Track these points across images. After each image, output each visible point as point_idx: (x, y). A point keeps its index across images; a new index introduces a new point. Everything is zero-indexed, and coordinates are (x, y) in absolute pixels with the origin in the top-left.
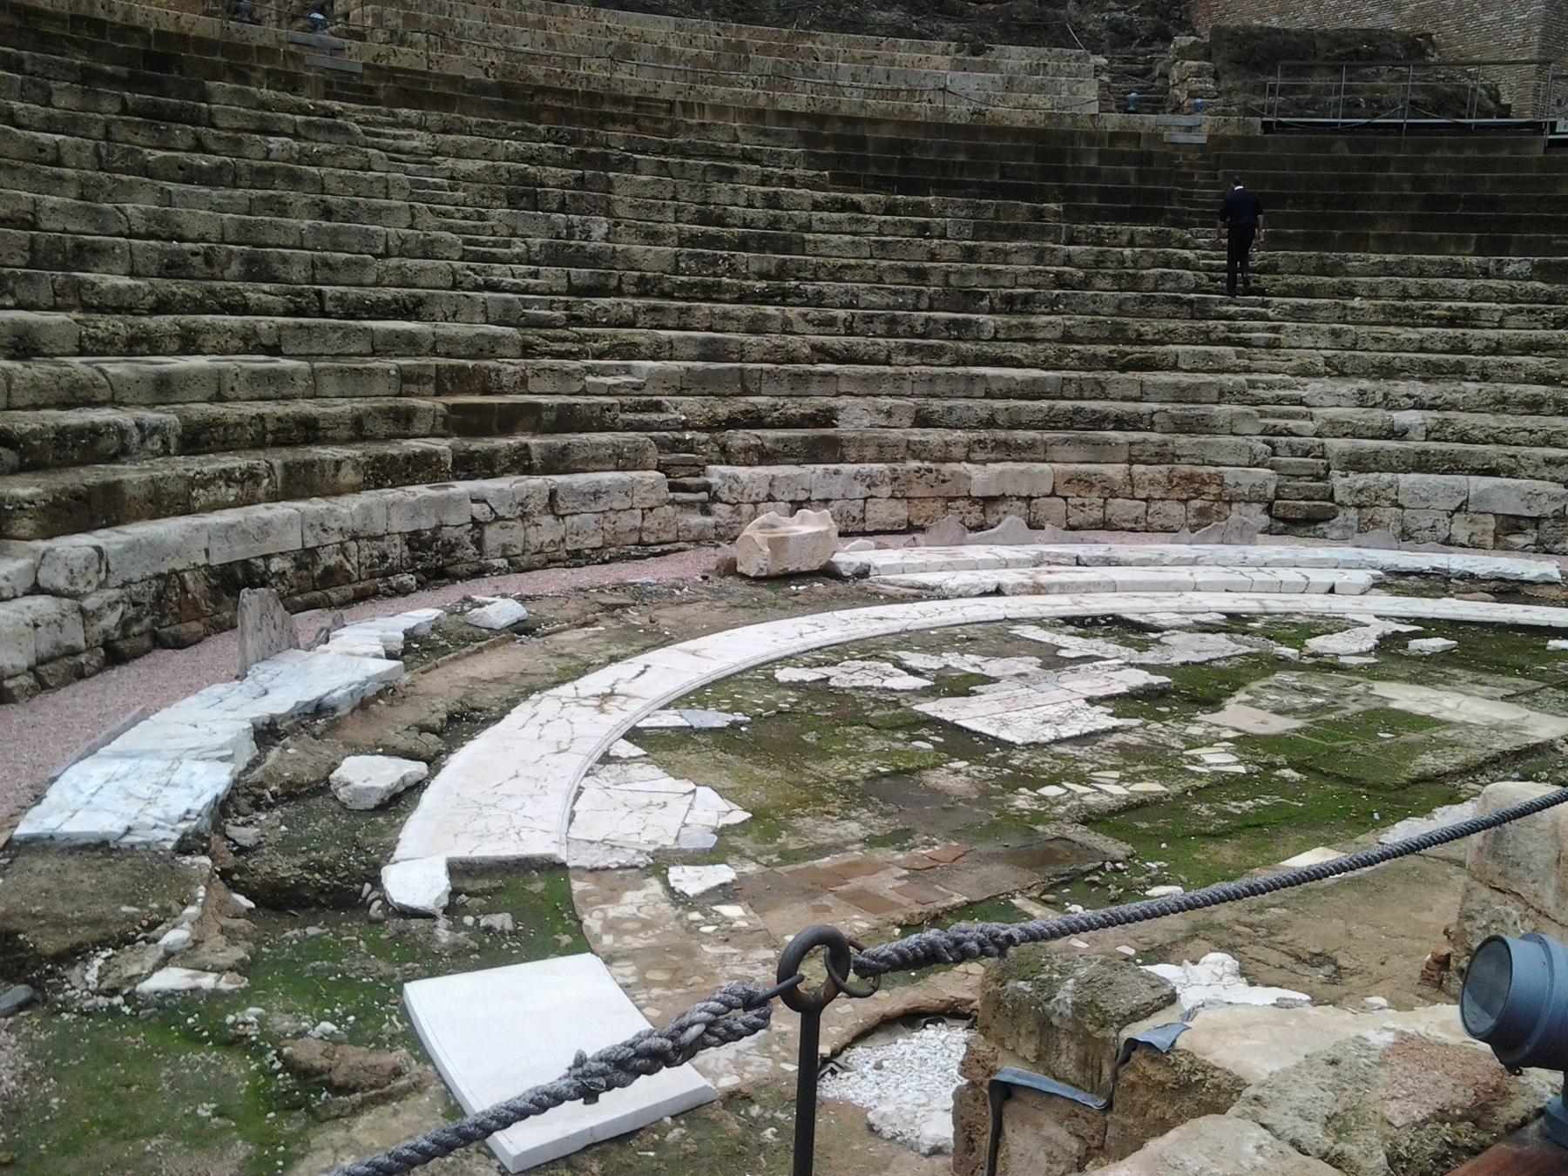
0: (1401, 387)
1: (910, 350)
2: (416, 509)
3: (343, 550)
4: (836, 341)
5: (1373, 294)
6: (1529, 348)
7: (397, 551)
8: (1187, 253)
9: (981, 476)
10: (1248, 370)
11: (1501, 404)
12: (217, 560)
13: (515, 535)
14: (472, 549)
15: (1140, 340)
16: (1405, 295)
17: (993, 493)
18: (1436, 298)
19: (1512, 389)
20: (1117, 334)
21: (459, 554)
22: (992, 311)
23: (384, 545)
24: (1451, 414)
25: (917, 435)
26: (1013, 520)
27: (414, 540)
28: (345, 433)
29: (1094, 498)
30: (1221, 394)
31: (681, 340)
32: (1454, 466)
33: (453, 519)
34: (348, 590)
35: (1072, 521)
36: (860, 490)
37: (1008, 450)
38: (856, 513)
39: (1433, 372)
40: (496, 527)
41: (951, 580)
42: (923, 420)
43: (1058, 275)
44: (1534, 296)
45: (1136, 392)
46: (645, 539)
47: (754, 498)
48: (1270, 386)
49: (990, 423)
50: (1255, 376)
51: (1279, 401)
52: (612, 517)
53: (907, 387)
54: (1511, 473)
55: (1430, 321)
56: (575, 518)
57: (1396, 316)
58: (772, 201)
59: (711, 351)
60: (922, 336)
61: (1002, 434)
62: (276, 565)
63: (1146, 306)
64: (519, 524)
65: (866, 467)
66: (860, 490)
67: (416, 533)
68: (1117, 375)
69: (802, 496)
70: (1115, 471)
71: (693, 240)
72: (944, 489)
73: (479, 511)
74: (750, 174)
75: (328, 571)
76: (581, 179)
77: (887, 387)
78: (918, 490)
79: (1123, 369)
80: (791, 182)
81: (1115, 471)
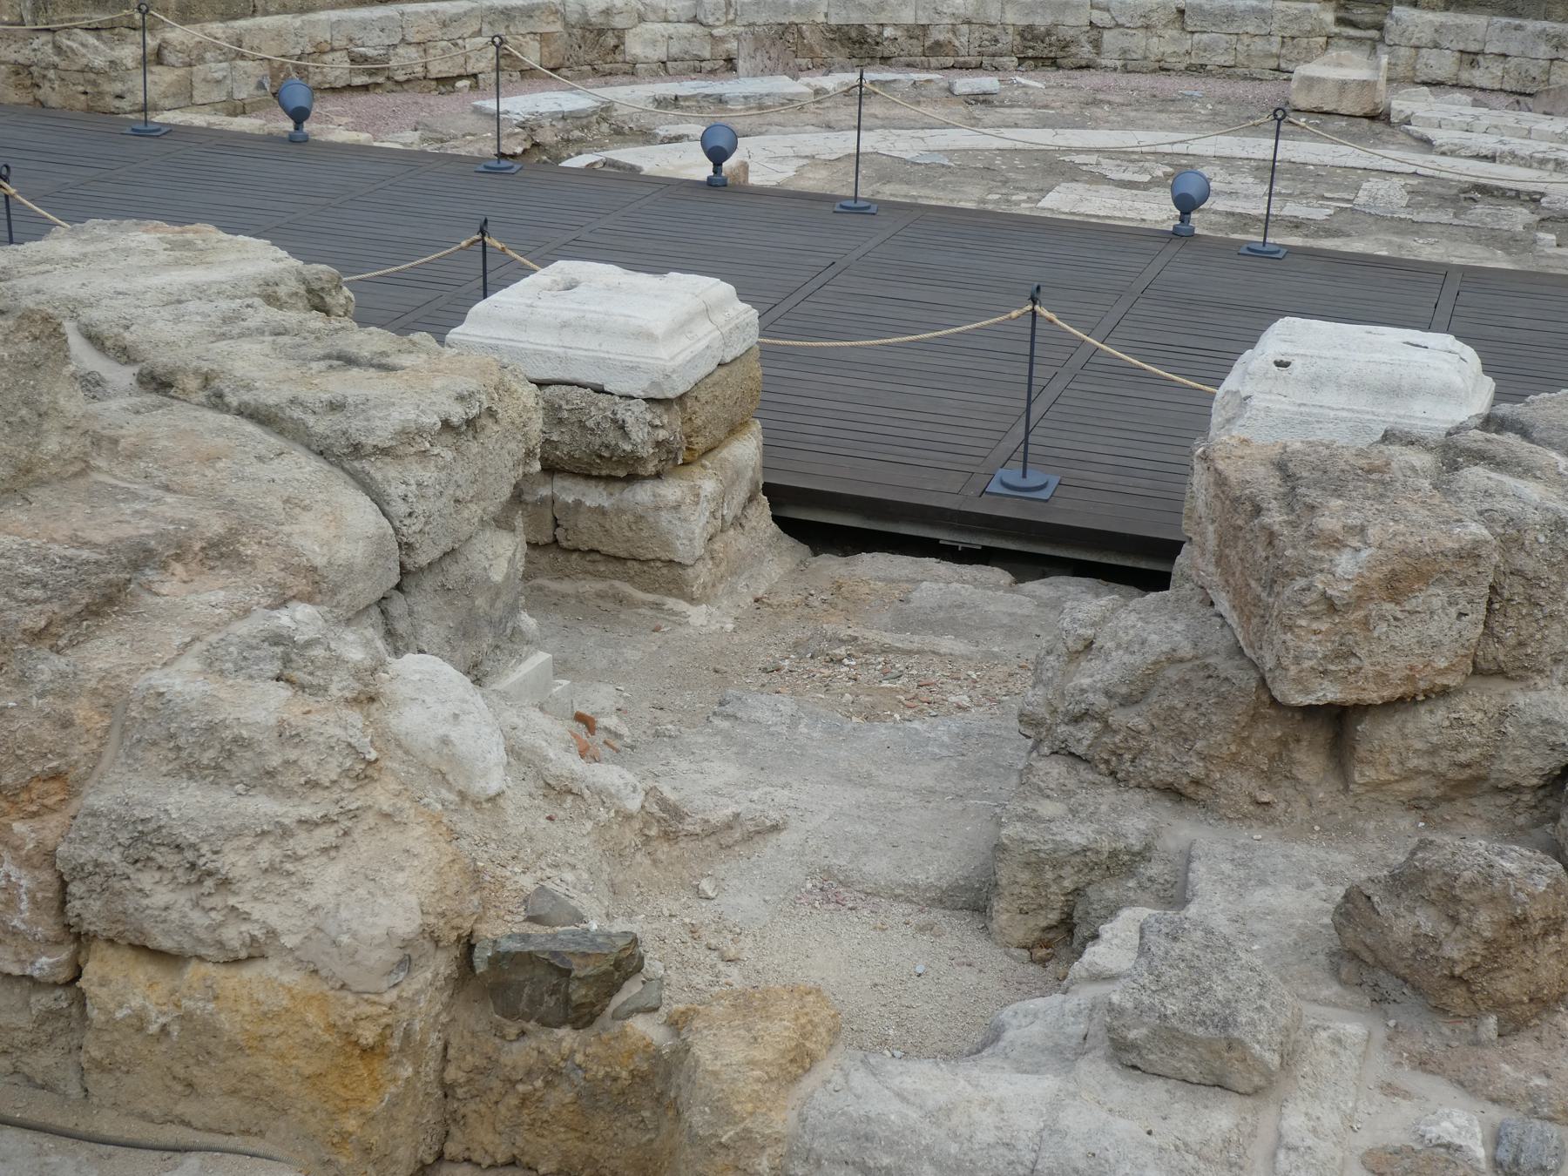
3: (954, 30)
7: (1009, 40)
12: (833, 21)
13: (1137, 41)
14: (1088, 47)
21: (1073, 50)
23: (995, 32)
27: (1028, 34)
33: (1070, 21)
34: (950, 61)
36: (1544, 50)
38: (1534, 72)
40: (1116, 32)
41: (1440, 137)
46: (1283, 66)
47: (1414, 42)
52: (1246, 39)
56: (1205, 36)
62: (888, 32)
64: (1140, 33)
66: (1544, 50)
67: (1030, 27)
69: (1473, 47)
73: (1097, 16)
75: (938, 44)
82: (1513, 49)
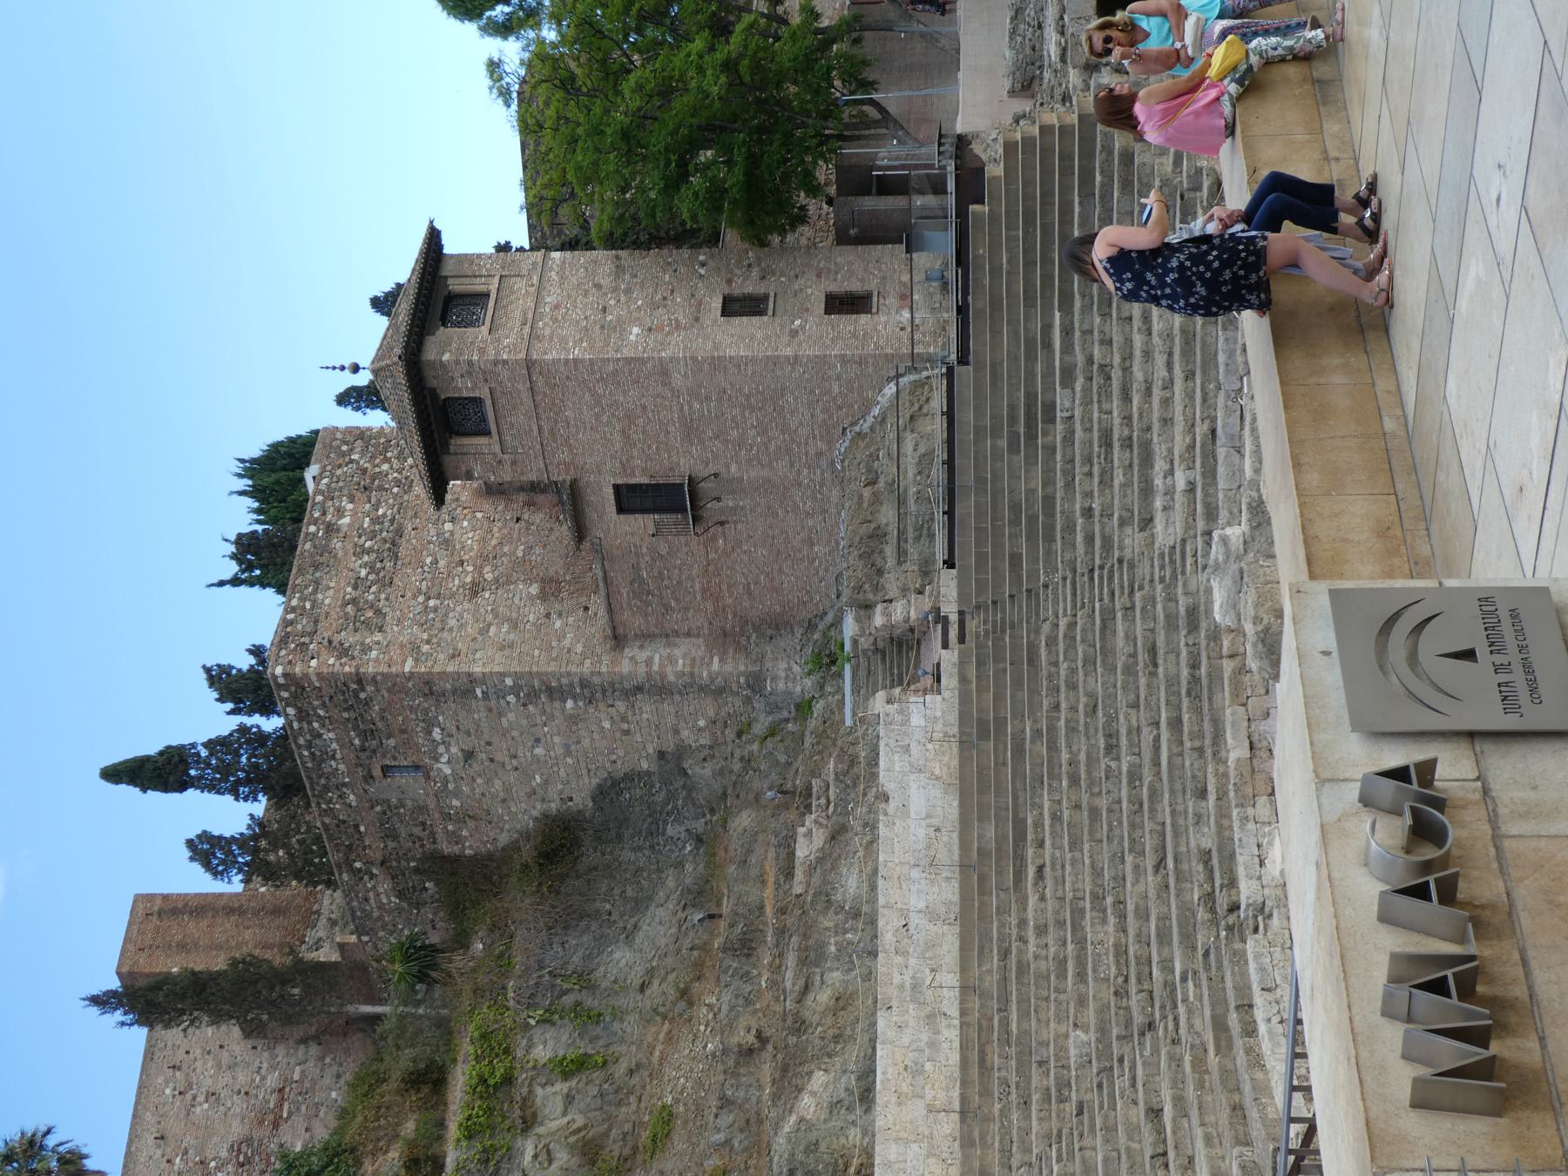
0: (1158, 482)
1: (1152, 810)
2: (1276, 1044)
4: (1150, 862)
5: (1088, 495)
6: (1126, 397)
8: (1063, 623)
9: (1236, 752)
10: (1152, 581)
11: (1167, 422)
15: (1134, 655)
16: (1090, 474)
17: (1247, 745)
18: (1091, 453)
19: (1156, 415)
20: (1130, 670)
22: (1118, 759)
24: (1177, 454)
25: (1212, 797)
26: (1263, 726)
28: (1236, 1097)
29: (1246, 679)
30: (1170, 600)
31: (1160, 954)
32: (1210, 457)
35: (1263, 691)
36: (1251, 826)
37: (1218, 737)
39: (1147, 460)
42: (1202, 793)
43: (1086, 715)
44: (1087, 391)
45: (1172, 657)
48: (1162, 567)
49: (1200, 751)
50: (1157, 578)
51: (1172, 561)
53: (1180, 808)
54: (1214, 420)
55: (1109, 458)
57: (1106, 482)
58: (1041, 930)
59: (1164, 936)
60: (1141, 805)
61: (1208, 742)
63: (1108, 652)
65: (1236, 825)
66: (1251, 826)
68: (1161, 670)
69: (1257, 860)
70: (1228, 666)
71: (1081, 976)
72: (1247, 775)
73: (1275, 1020)
74: (1019, 951)
76: (1040, 1063)
77: (1181, 821)
78: (1249, 790)
79: (1156, 665)
80: (1023, 923)
81: (1228, 666)
82: (1253, 840)
